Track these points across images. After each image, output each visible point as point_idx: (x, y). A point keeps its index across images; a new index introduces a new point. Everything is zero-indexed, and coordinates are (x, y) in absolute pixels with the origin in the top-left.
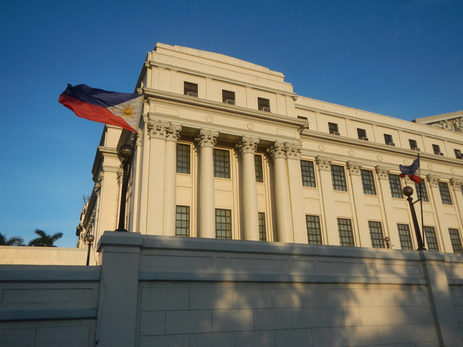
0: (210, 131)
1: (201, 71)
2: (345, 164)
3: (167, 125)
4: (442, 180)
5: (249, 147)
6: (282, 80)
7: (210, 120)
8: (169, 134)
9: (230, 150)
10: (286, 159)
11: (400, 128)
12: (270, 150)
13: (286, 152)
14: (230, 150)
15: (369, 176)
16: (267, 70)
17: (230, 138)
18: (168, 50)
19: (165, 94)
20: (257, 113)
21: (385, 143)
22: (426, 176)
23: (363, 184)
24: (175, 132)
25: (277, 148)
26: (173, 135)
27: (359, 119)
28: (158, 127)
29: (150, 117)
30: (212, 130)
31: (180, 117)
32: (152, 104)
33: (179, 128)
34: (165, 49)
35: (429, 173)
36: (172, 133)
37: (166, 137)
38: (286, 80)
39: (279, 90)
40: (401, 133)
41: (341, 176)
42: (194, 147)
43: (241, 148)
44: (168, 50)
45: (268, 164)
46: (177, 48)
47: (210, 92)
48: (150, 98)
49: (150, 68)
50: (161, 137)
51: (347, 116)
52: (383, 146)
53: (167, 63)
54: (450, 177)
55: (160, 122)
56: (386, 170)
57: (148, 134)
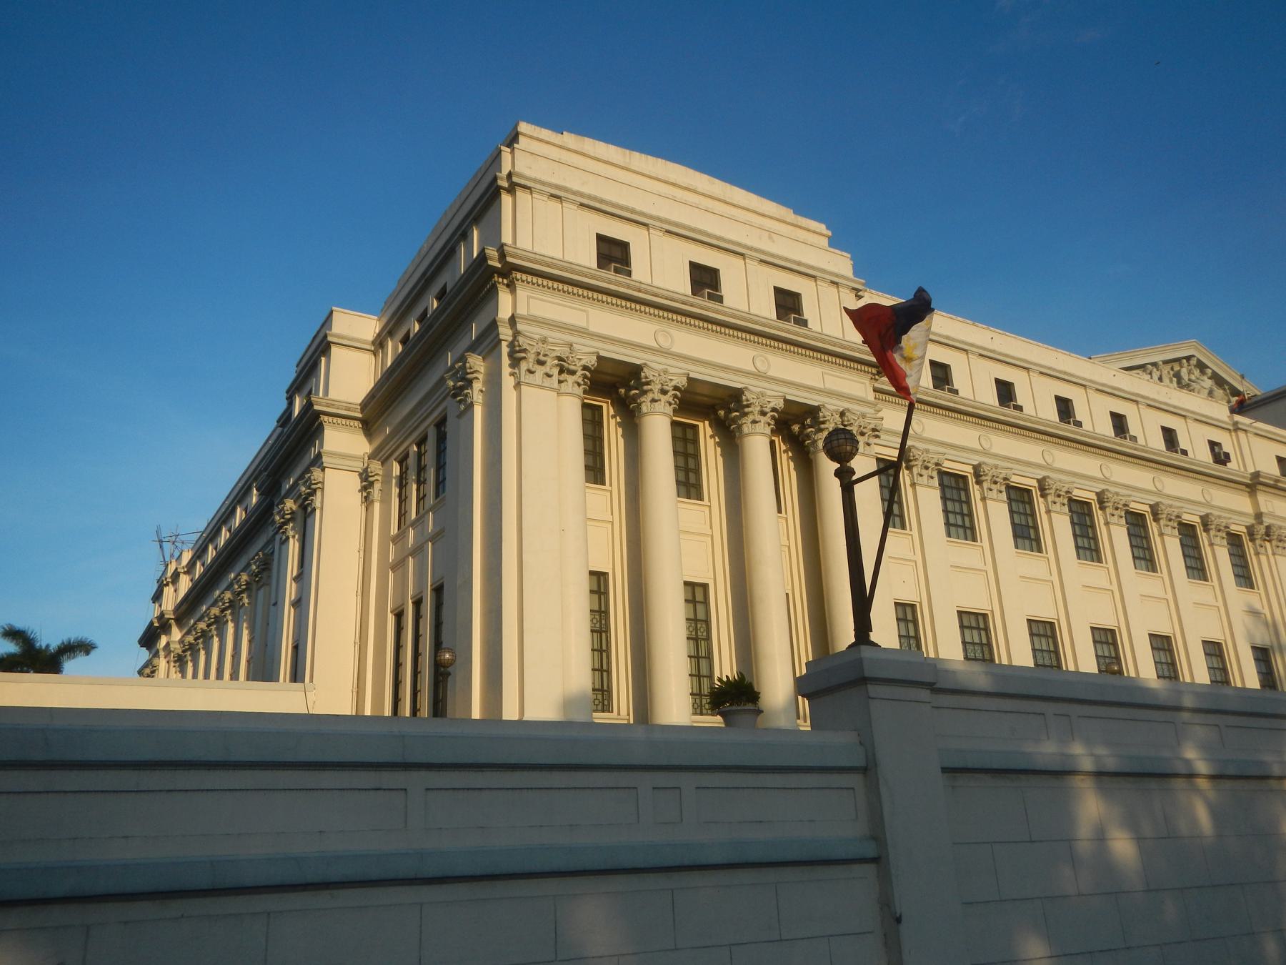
0: (666, 372)
1: (638, 208)
2: (970, 469)
3: (561, 351)
4: (1135, 507)
5: (758, 417)
7: (665, 343)
8: (564, 376)
9: (701, 425)
11: (1090, 381)
12: (803, 427)
14: (701, 425)
15: (959, 489)
17: (699, 390)
18: (548, 143)
19: (578, 273)
20: (770, 327)
21: (997, 404)
22: (1151, 506)
23: (1013, 524)
24: (580, 373)
25: (823, 423)
26: (575, 378)
27: (1000, 354)
28: (539, 354)
29: (520, 327)
30: (672, 370)
31: (592, 329)
32: (522, 292)
33: (592, 361)
34: (541, 140)
35: (1157, 499)
36: (573, 373)
37: (560, 382)
38: (834, 243)
39: (824, 271)
40: (1092, 394)
41: (960, 501)
42: (612, 412)
43: (734, 420)
44: (548, 143)
45: (792, 464)
46: (569, 139)
47: (660, 267)
48: (519, 275)
49: (512, 189)
50: (547, 382)
51: (972, 345)
52: (1108, 442)
53: (554, 181)
55: (544, 341)
56: (1065, 489)
57: (512, 374)
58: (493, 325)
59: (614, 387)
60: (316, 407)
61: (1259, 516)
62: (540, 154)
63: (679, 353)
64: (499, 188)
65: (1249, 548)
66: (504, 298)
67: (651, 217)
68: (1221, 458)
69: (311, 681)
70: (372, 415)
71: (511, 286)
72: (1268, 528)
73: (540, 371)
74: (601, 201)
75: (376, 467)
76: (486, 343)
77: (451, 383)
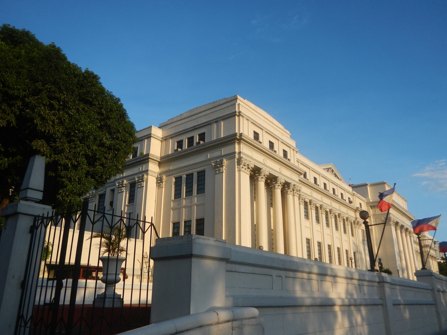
2: (308, 201)
6: (289, 136)
10: (294, 195)
13: (293, 190)
29: (242, 155)
32: (242, 145)
38: (292, 137)
40: (331, 184)
46: (245, 101)
49: (239, 115)
54: (347, 216)
55: (246, 160)
58: (235, 152)
59: (255, 173)
60: (150, 157)
62: (244, 106)
63: (270, 166)
64: (236, 115)
65: (353, 226)
66: (237, 146)
67: (264, 127)
68: (350, 202)
70: (164, 161)
71: (239, 143)
72: (358, 221)
73: (245, 167)
74: (256, 122)
75: (164, 177)
76: (229, 157)
77: (214, 165)
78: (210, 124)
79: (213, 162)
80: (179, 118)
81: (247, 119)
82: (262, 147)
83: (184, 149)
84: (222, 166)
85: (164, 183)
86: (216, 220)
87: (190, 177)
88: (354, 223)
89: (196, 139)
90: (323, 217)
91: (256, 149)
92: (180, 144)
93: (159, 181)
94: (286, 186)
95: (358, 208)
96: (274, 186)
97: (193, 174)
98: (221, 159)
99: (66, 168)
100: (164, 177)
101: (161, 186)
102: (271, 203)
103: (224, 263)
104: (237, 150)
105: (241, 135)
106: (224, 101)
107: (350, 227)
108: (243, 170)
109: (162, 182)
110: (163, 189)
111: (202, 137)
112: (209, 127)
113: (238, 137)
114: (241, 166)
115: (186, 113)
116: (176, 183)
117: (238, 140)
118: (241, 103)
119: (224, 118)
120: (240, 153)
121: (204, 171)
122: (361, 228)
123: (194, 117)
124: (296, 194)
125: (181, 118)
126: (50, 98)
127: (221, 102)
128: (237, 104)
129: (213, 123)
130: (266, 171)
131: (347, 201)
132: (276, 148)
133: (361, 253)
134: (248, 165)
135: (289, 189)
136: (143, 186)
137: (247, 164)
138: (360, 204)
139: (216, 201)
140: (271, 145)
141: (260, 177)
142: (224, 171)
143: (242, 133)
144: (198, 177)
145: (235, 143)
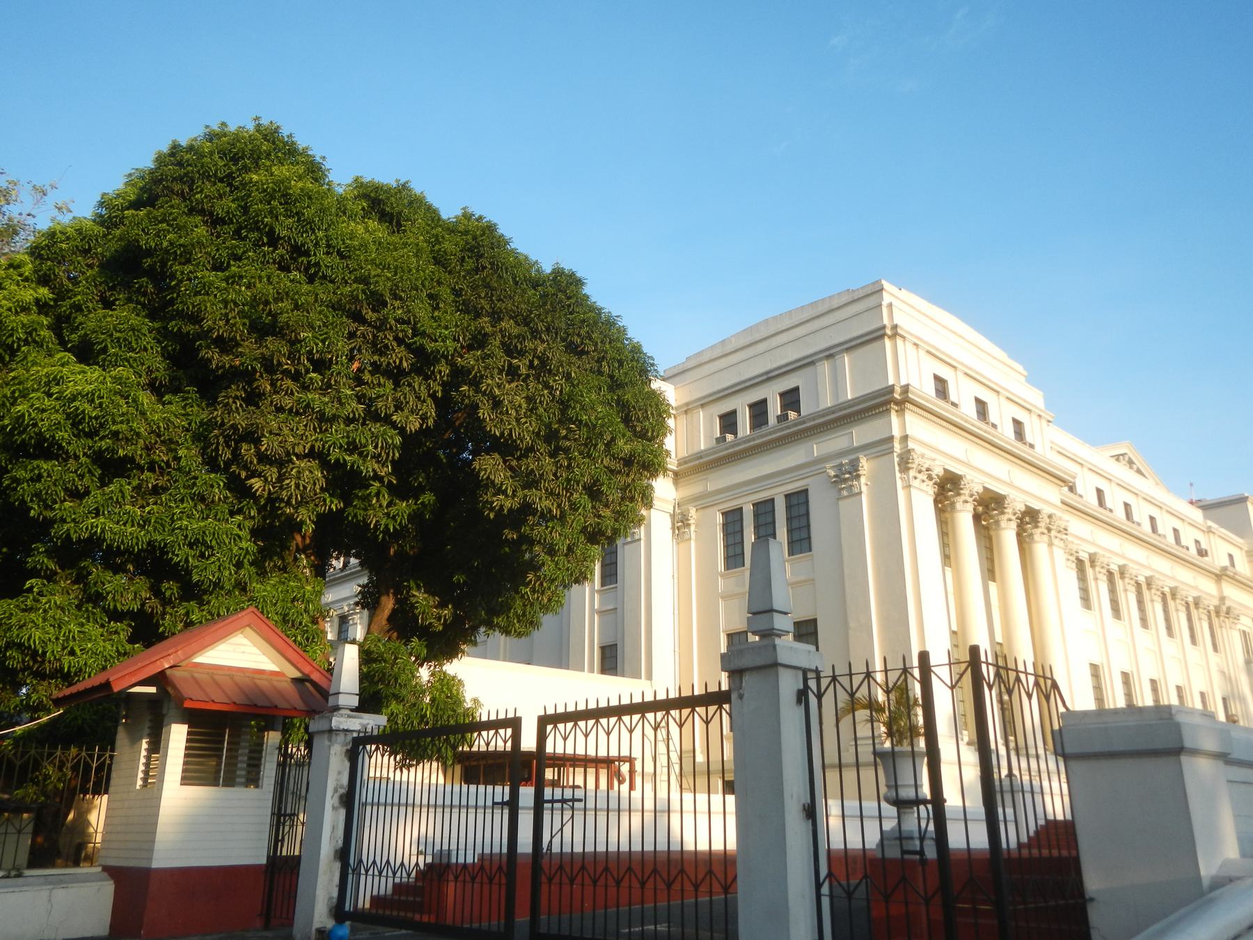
6: (1023, 379)
10: (1051, 544)
13: (1049, 530)
16: (1002, 355)
29: (911, 445)
32: (909, 417)
38: (1029, 380)
46: (904, 294)
48: (908, 405)
54: (1196, 594)
55: (923, 456)
58: (891, 438)
61: (1222, 599)
62: (904, 307)
63: (983, 470)
65: (1215, 620)
66: (894, 417)
68: (1202, 553)
69: (649, 677)
71: (901, 412)
73: (920, 476)
74: (937, 350)
75: (693, 512)
76: (874, 450)
77: (832, 473)
78: (812, 363)
79: (832, 468)
80: (718, 353)
81: (915, 344)
82: (962, 418)
83: (740, 434)
84: (858, 476)
85: (693, 528)
86: (852, 624)
87: (764, 510)
88: (1218, 613)
89: (775, 408)
90: (1129, 600)
91: (945, 424)
92: (728, 423)
93: (680, 523)
94: (1030, 517)
95: (1225, 569)
96: (997, 523)
97: (773, 500)
98: (853, 457)
99: (546, 516)
100: (693, 512)
101: (687, 537)
102: (991, 570)
103: (1220, 764)
104: (896, 432)
105: (906, 389)
106: (844, 299)
107: (1206, 625)
108: (916, 483)
109: (689, 525)
110: (693, 543)
111: (791, 399)
112: (809, 370)
113: (897, 396)
114: (912, 473)
115: (737, 335)
116: (725, 526)
117: (897, 403)
118: (896, 303)
119: (852, 345)
120: (905, 438)
121: (805, 492)
122: (1239, 626)
123: (761, 347)
124: (1056, 542)
125: (724, 352)
126: (509, 351)
127: (836, 303)
128: (885, 303)
129: (821, 359)
130: (974, 483)
131: (1193, 551)
132: (993, 416)
133: (1242, 700)
134: (928, 470)
135: (1037, 527)
136: (639, 540)
137: (926, 466)
138: (1231, 556)
139: (846, 571)
140: (981, 406)
141: (960, 500)
142: (864, 489)
143: (908, 385)
144: (789, 507)
145: (888, 411)
